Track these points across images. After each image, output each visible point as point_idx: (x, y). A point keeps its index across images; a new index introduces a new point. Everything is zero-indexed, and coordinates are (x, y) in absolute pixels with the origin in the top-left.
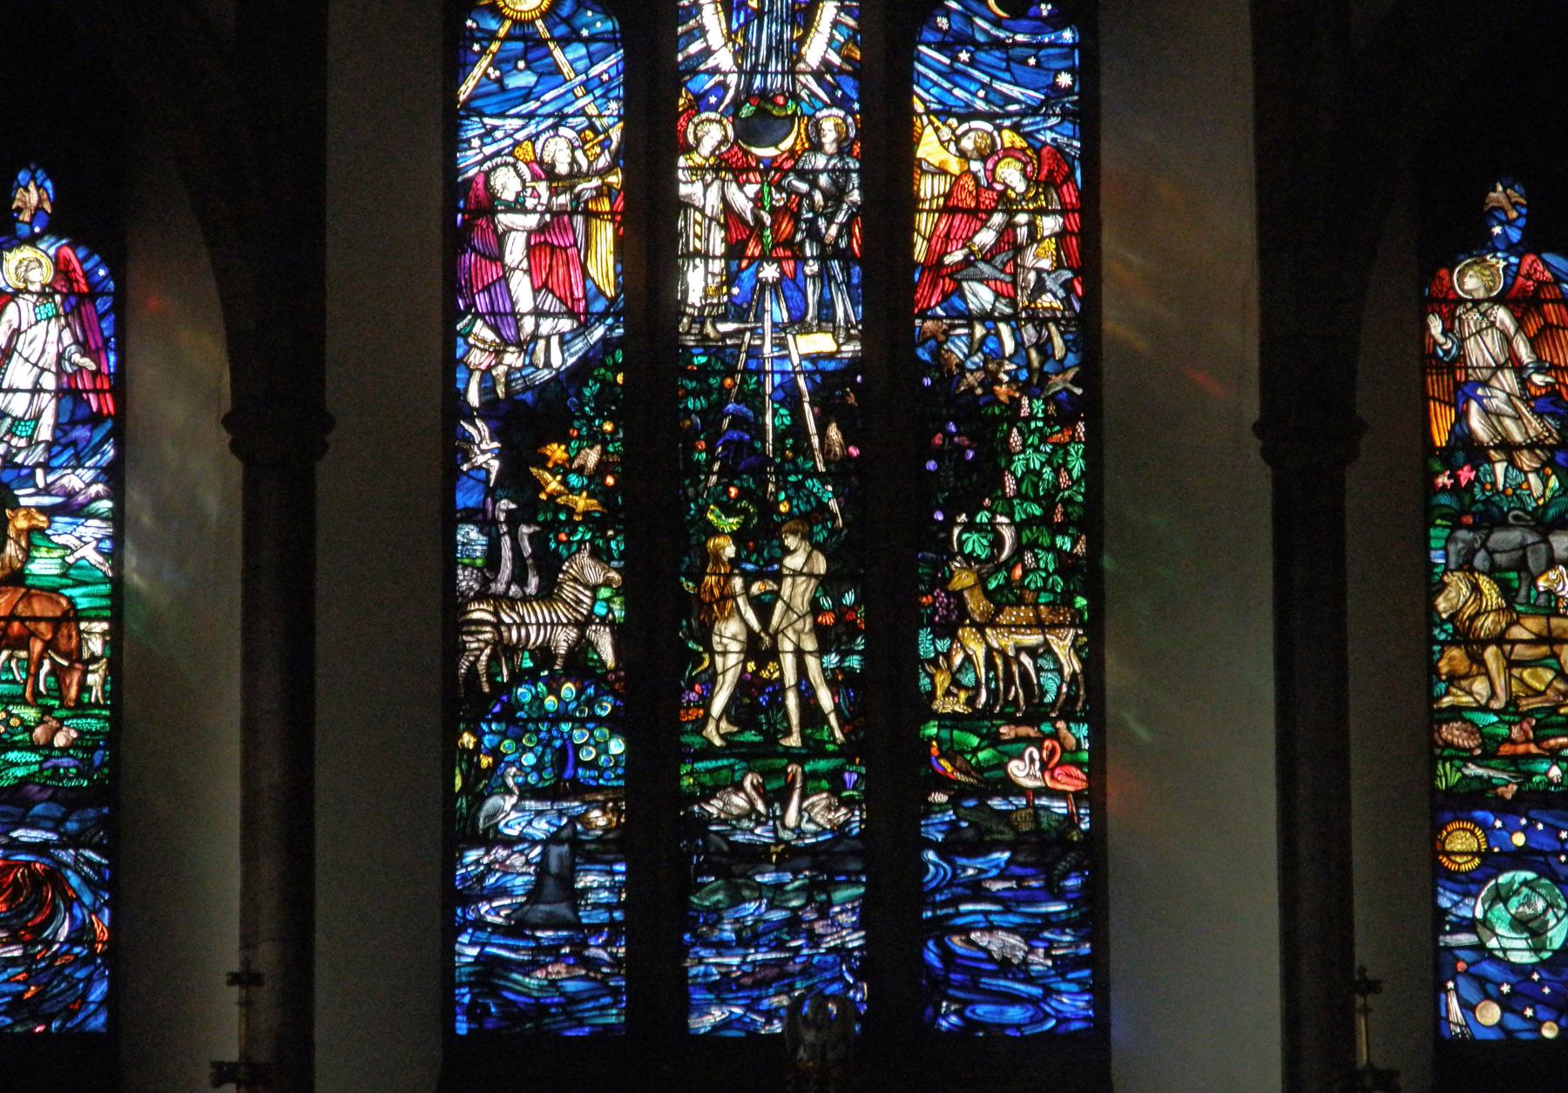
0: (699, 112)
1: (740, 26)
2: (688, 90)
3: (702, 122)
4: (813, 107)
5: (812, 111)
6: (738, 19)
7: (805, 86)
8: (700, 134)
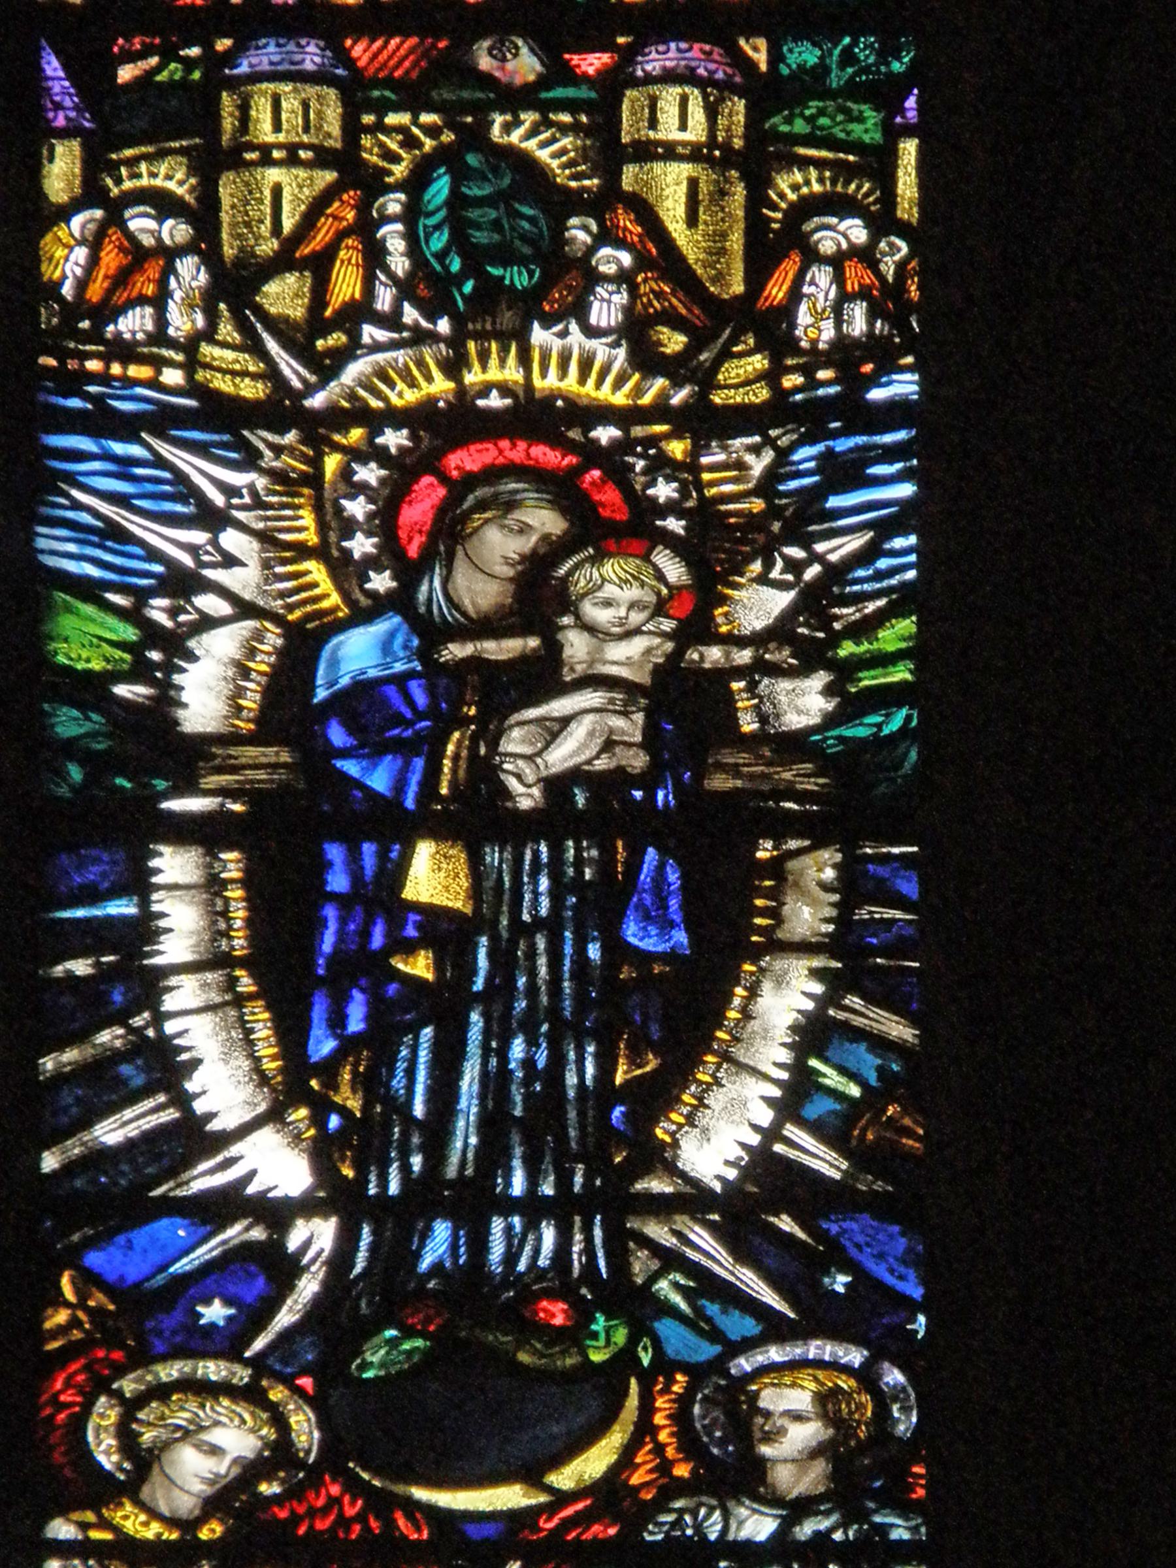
0: (143, 1358)
1: (348, 1046)
2: (88, 1280)
3: (161, 1392)
4: (715, 1335)
5: (708, 1351)
6: (337, 1021)
7: (670, 1260)
8: (148, 1437)
